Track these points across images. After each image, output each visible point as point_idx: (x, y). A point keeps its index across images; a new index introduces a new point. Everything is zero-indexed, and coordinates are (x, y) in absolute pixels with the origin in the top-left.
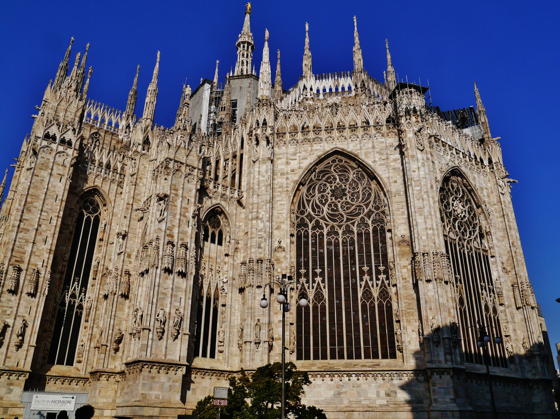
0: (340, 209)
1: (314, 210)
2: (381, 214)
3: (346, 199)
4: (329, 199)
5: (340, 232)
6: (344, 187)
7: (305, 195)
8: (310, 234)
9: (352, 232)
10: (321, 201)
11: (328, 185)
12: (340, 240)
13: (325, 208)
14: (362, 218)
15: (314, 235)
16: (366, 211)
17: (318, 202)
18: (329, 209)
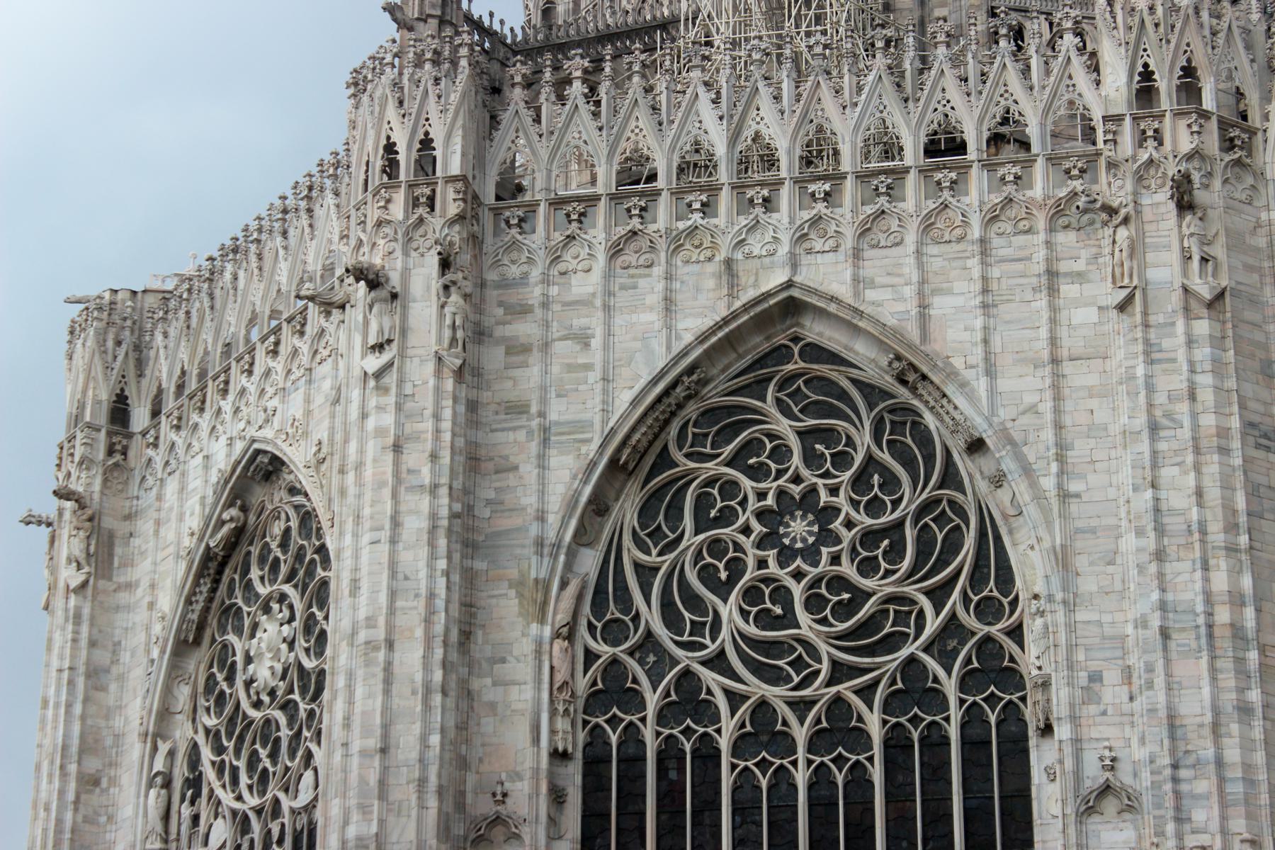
0: (802, 616)
1: (671, 619)
2: (1009, 645)
3: (836, 559)
4: (751, 562)
5: (801, 734)
6: (824, 497)
7: (627, 541)
8: (651, 747)
9: (859, 738)
10: (707, 575)
11: (747, 484)
12: (801, 777)
13: (729, 610)
14: (912, 660)
15: (669, 754)
16: (932, 624)
17: (692, 577)
18: (744, 614)
